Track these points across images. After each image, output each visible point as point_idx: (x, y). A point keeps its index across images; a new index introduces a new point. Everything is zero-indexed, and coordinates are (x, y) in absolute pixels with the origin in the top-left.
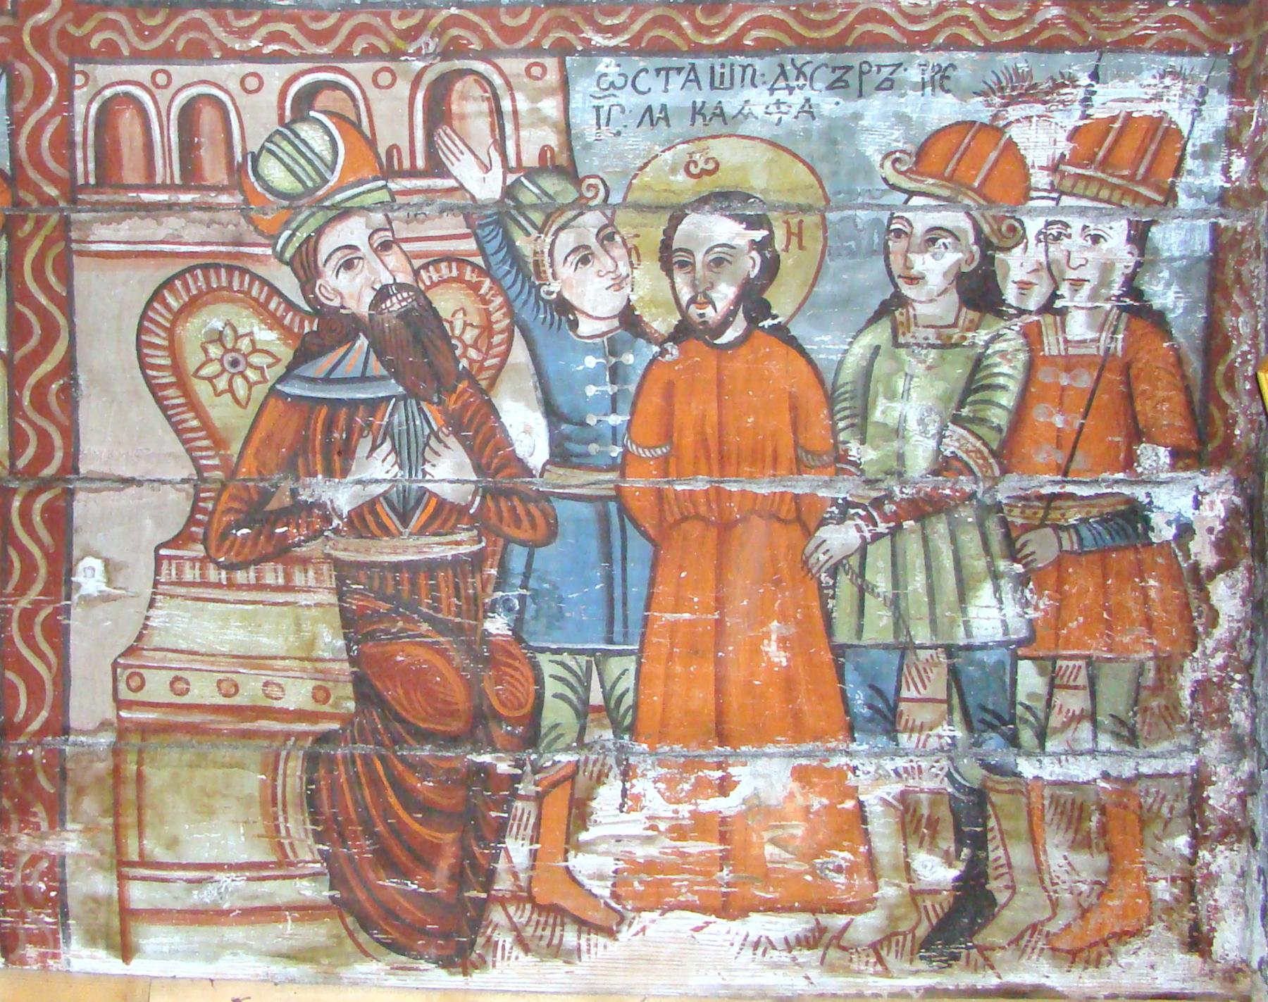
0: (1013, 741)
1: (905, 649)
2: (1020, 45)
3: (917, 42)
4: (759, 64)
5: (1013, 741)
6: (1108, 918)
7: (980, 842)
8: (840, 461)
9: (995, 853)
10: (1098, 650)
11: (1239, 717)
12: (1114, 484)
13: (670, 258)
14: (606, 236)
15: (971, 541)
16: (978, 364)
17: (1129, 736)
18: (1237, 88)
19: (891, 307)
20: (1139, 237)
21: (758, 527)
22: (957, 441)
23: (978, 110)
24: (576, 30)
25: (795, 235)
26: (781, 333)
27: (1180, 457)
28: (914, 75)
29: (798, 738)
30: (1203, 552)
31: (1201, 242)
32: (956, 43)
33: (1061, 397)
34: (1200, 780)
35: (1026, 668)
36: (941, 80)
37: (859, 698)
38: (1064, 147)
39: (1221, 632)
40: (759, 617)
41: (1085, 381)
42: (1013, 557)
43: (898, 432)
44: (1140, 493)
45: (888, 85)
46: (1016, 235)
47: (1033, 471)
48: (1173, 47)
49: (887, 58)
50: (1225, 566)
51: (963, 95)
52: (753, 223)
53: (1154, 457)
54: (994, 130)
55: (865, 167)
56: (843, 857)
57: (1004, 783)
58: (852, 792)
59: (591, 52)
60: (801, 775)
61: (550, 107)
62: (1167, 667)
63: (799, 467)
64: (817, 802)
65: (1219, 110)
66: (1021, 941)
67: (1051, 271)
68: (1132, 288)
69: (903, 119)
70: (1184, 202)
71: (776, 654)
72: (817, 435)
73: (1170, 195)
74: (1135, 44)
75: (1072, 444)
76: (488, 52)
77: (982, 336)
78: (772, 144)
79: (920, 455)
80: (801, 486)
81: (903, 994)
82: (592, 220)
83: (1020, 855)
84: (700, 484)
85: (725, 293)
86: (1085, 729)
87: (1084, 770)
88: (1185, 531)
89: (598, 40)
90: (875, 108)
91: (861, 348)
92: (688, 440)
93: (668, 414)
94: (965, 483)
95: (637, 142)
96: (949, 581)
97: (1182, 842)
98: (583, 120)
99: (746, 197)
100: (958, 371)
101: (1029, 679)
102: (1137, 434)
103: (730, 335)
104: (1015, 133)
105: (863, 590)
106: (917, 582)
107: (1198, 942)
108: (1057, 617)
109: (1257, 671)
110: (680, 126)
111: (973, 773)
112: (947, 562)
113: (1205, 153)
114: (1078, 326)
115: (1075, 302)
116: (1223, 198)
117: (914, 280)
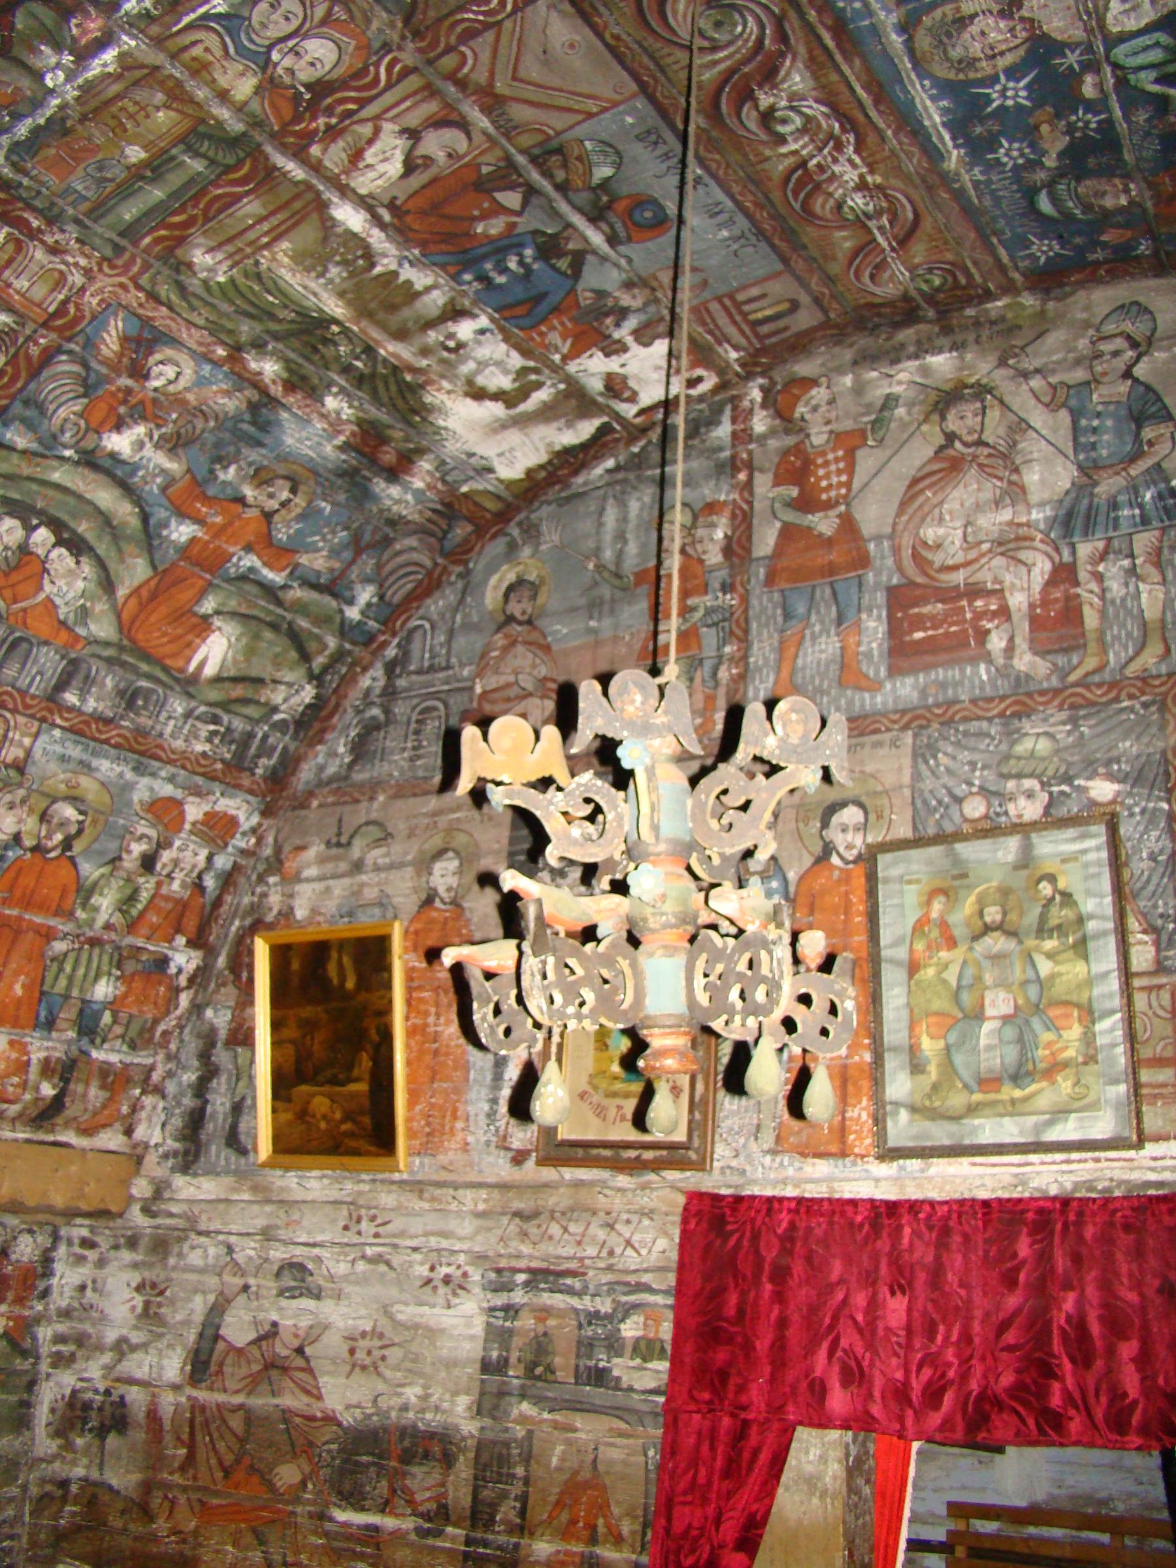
0: (92, 1042)
1: (67, 997)
2: (203, 775)
3: (170, 762)
4: (113, 751)
5: (92, 1042)
6: (101, 1119)
7: (67, 1081)
8: (71, 915)
9: (72, 1086)
10: (135, 1011)
11: (173, 1046)
12: (163, 948)
13: (44, 817)
14: (23, 801)
15: (106, 958)
16: (136, 891)
17: (133, 1046)
18: (266, 813)
19: (116, 860)
20: (210, 859)
21: (31, 935)
22: (118, 919)
23: (179, 794)
24: (52, 712)
25: (95, 822)
26: (72, 859)
27: (191, 944)
28: (163, 774)
29: (14, 1026)
30: (183, 981)
31: (229, 866)
32: (184, 767)
33: (159, 911)
34: (152, 1068)
35: (107, 1013)
36: (171, 779)
37: (43, 1014)
38: (200, 817)
39: (178, 1012)
40: (17, 974)
41: (170, 906)
42: (119, 967)
43: (96, 909)
44: (170, 953)
45: (153, 775)
46: (169, 845)
47: (137, 935)
48: (251, 792)
49: (156, 764)
50: (188, 987)
51: (176, 786)
52: (81, 812)
53: (181, 940)
54: (178, 804)
55: (129, 804)
56: (16, 1080)
57: (83, 1058)
58: (27, 1053)
59: (54, 725)
60: (12, 1043)
61: (27, 741)
62: (156, 1022)
63: (56, 914)
64: (14, 1055)
65: (255, 819)
66: (67, 1125)
67: (176, 862)
68: (200, 877)
69: (152, 789)
70: (230, 849)
71: (18, 990)
72: (67, 905)
73: (226, 845)
74: (238, 787)
75: (154, 929)
76: (14, 711)
77: (142, 880)
78: (103, 784)
79: (101, 919)
80: (52, 922)
81: (16, 1140)
82: (21, 792)
83: (80, 1088)
84: (14, 912)
85: (59, 837)
86: (119, 1042)
87: (114, 1058)
88: (180, 971)
89: (59, 721)
90: (145, 781)
91: (97, 874)
92: (18, 893)
93: (16, 879)
94: (113, 936)
95: (53, 766)
96: (92, 974)
97: (137, 1092)
98: (37, 753)
99: (83, 801)
100: (128, 891)
101: (107, 1018)
102: (178, 930)
103: (52, 855)
104: (187, 807)
105: (61, 969)
106: (81, 971)
107: (129, 1132)
108: (125, 996)
109: (187, 1030)
110: (72, 766)
111: (74, 1051)
112: (95, 965)
113: (244, 834)
114: (176, 886)
115: (179, 876)
116: (243, 852)
117: (129, 852)
